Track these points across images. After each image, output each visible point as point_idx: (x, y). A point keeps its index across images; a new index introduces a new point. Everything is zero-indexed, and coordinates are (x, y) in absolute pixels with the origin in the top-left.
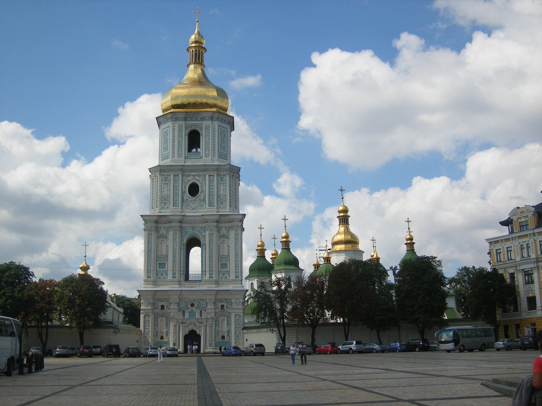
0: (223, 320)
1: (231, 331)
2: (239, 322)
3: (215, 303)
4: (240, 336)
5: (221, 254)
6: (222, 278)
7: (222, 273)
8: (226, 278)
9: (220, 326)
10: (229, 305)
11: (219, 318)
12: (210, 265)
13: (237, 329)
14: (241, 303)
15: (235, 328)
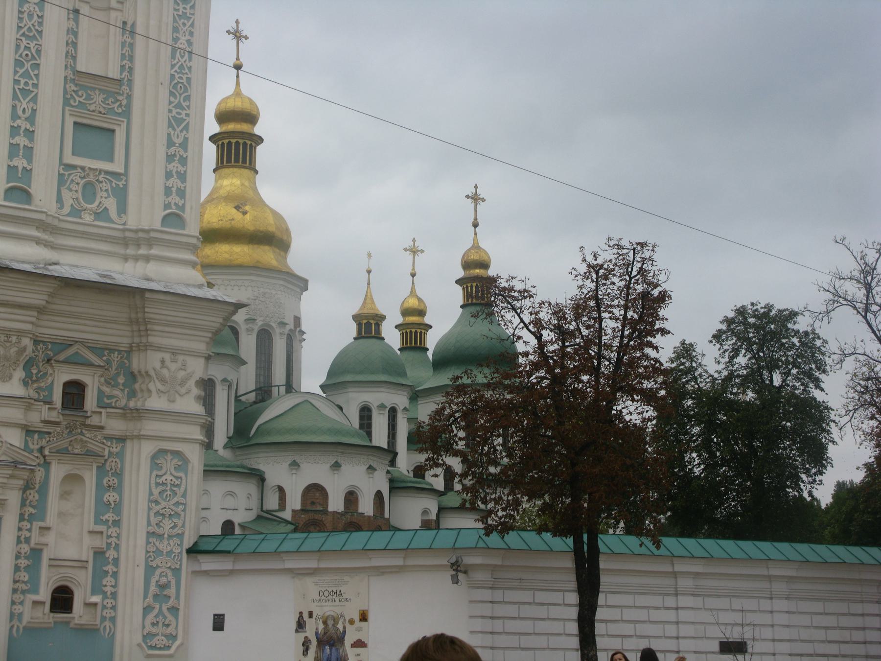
0: (73, 479)
1: (116, 561)
2: (177, 504)
3: (28, 365)
4: (172, 591)
5: (81, 67)
6: (76, 212)
7: (82, 182)
8: (102, 214)
9: (51, 519)
10: (116, 385)
11: (47, 464)
12: (14, 116)
13: (164, 546)
14: (191, 383)
15: (148, 543)
